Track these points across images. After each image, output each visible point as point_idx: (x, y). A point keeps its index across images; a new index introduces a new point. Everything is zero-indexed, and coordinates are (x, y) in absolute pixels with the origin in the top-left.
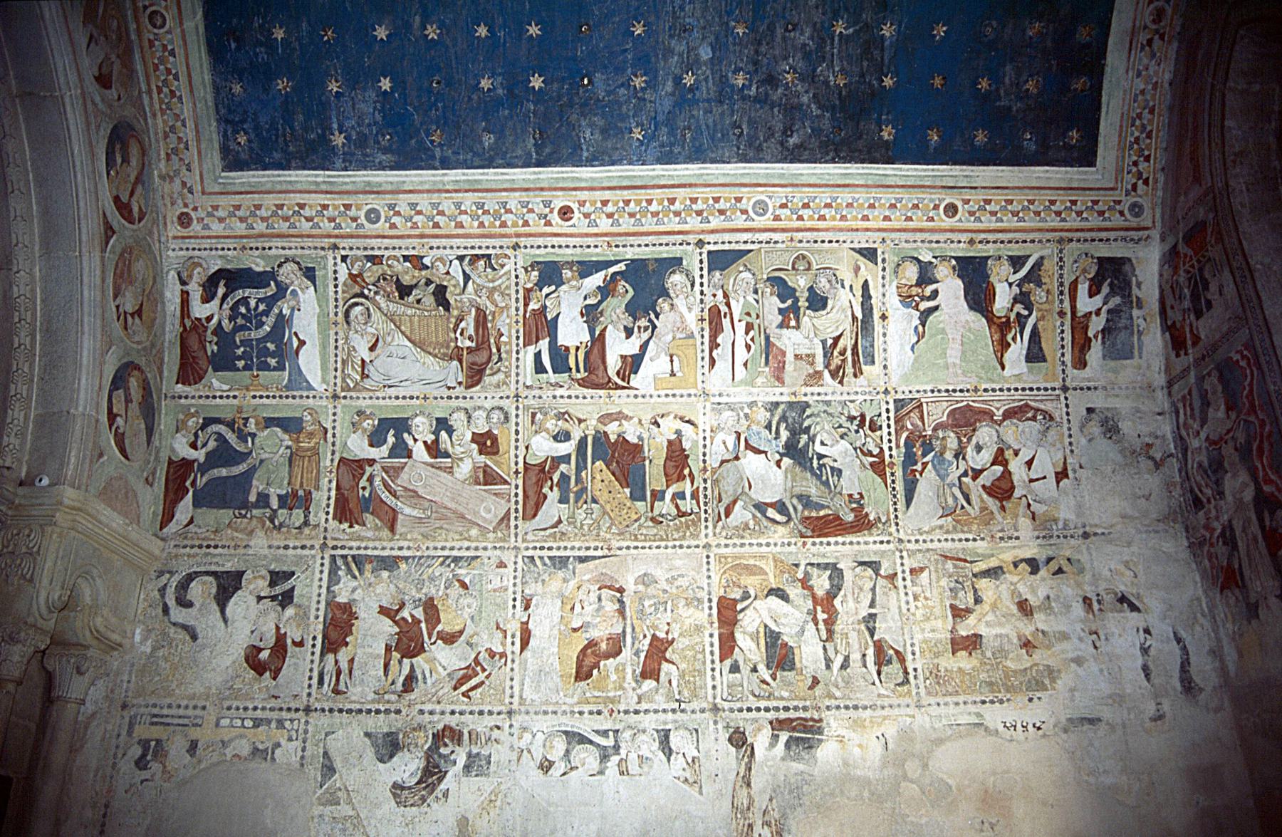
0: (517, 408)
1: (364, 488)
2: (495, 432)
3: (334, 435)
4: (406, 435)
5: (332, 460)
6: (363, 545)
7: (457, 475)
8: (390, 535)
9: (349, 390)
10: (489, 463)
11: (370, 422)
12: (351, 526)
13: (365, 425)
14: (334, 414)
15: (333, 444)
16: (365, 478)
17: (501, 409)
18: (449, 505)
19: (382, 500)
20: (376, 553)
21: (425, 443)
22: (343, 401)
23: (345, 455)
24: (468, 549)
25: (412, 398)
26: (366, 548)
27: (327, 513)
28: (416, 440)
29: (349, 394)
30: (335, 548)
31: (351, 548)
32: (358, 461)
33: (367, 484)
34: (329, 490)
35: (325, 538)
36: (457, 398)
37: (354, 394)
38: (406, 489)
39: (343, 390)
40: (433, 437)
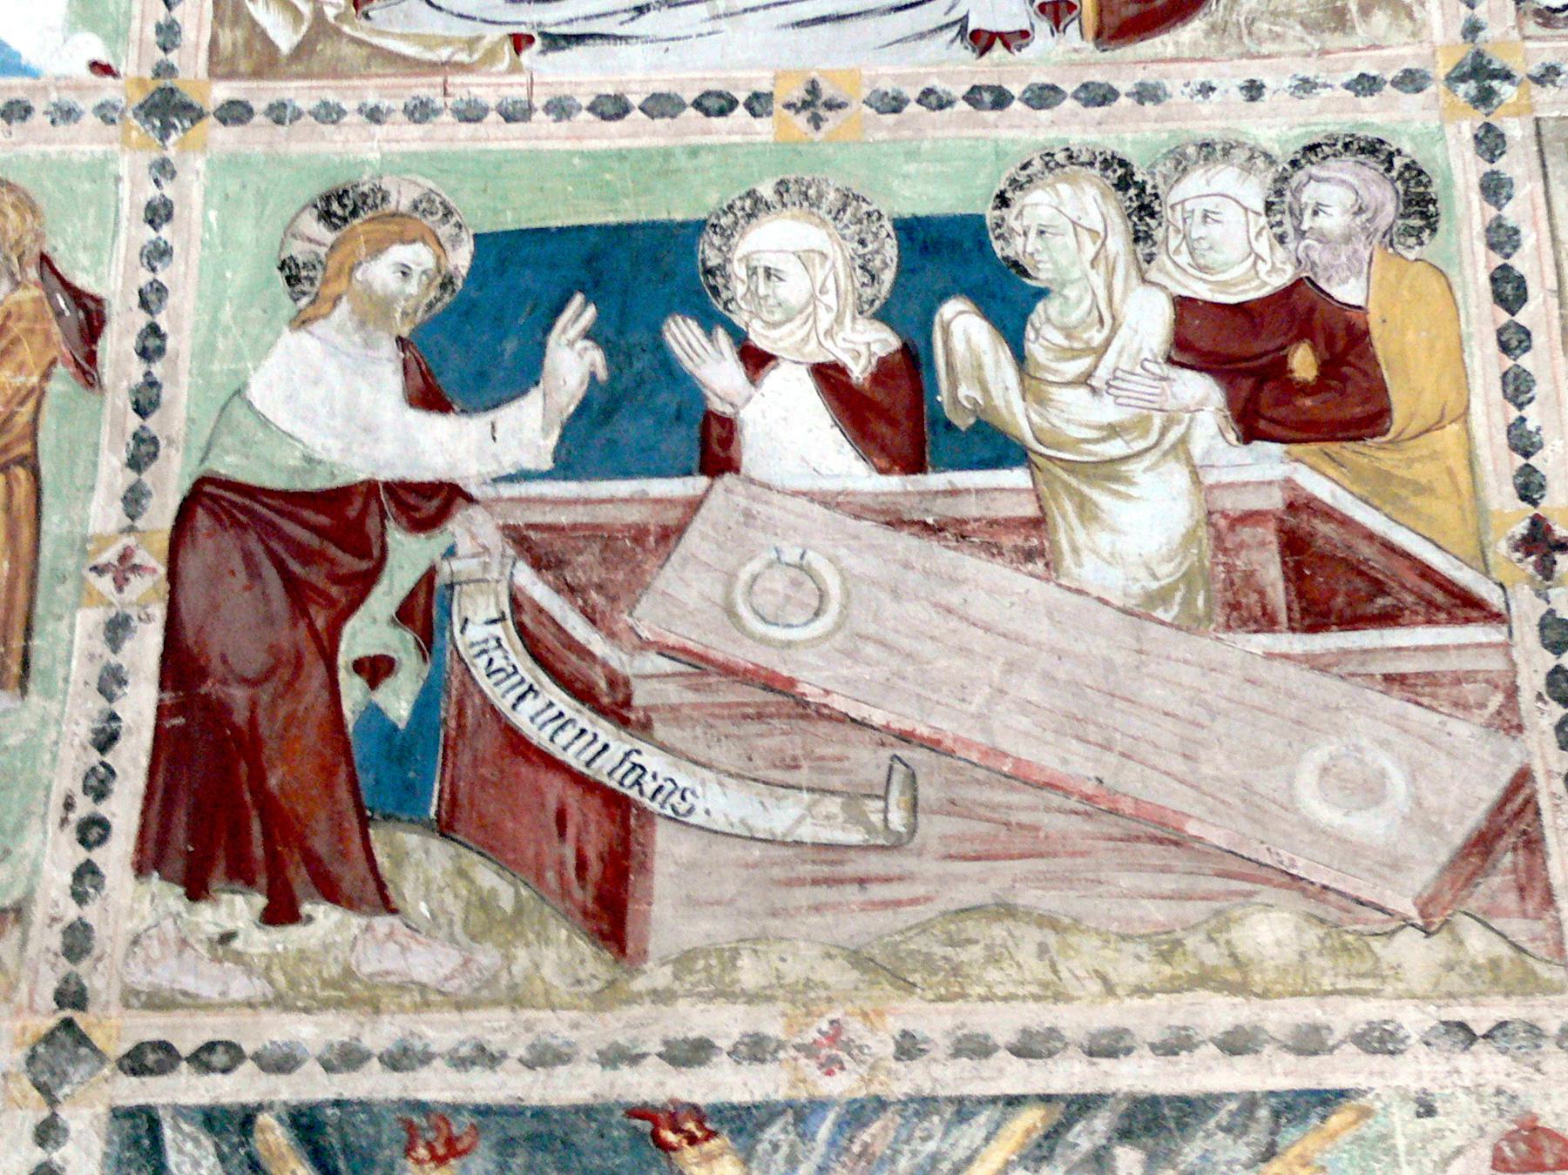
0: (1490, 142)
1: (376, 669)
2: (1347, 291)
3: (151, 345)
4: (682, 335)
5: (134, 500)
6: (381, 1035)
7: (1089, 571)
8: (592, 961)
9: (267, 62)
10: (1320, 487)
11: (419, 256)
12: (281, 912)
13: (381, 273)
14: (158, 214)
15: (146, 401)
16: (384, 599)
17: (1372, 148)
18: (1047, 758)
19: (517, 744)
20: (485, 1087)
21: (829, 377)
22: (223, 137)
23: (229, 465)
24: (1236, 1044)
25: (717, 104)
26: (400, 1059)
27: (93, 831)
28: (755, 360)
29: (261, 94)
30: (137, 1062)
31: (282, 1062)
32: (334, 499)
33: (400, 644)
34: (111, 681)
35: (72, 996)
36: (1044, 96)
37: (301, 93)
38: (698, 664)
39: (220, 66)
40: (882, 341)
